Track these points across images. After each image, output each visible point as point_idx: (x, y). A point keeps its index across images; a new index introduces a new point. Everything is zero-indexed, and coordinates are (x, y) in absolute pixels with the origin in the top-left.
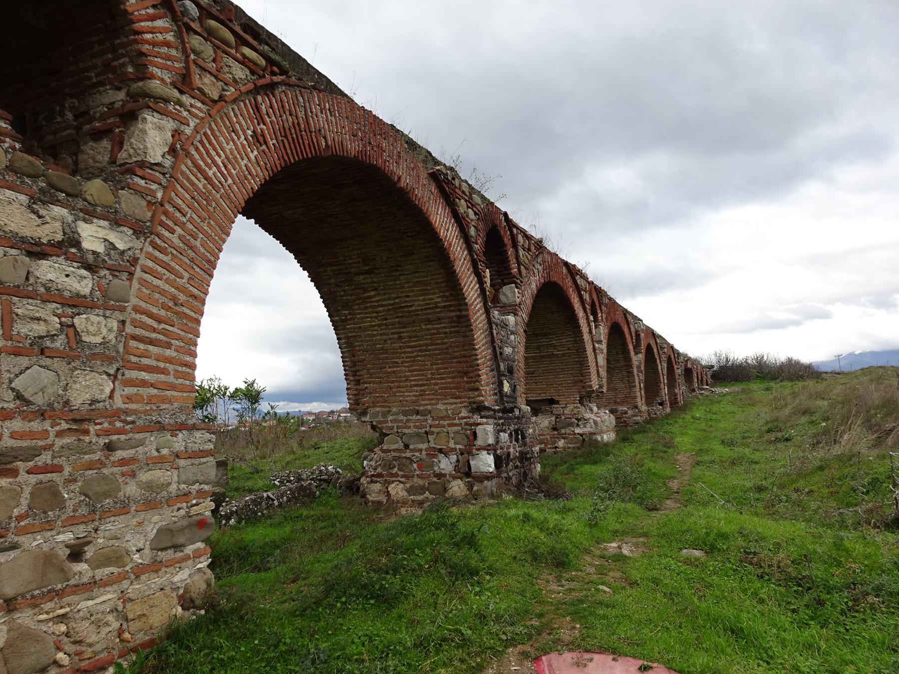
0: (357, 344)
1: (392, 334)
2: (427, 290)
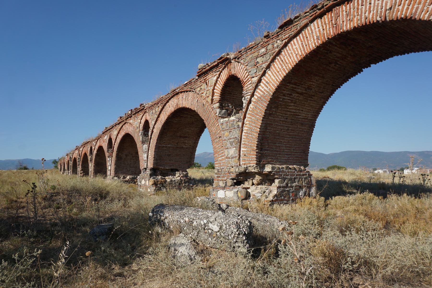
0: (269, 128)
1: (286, 127)
2: (311, 110)
